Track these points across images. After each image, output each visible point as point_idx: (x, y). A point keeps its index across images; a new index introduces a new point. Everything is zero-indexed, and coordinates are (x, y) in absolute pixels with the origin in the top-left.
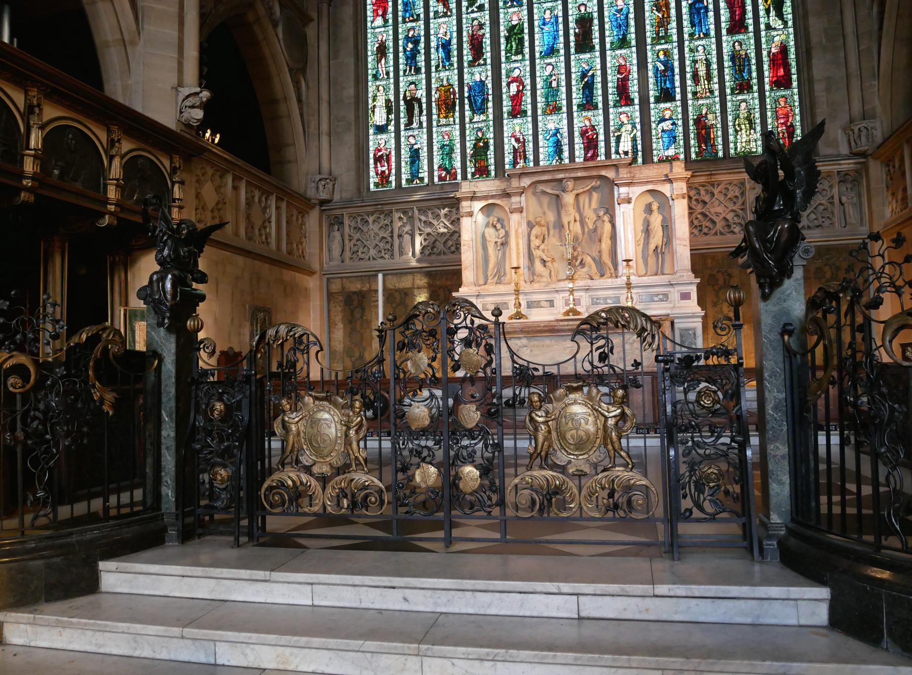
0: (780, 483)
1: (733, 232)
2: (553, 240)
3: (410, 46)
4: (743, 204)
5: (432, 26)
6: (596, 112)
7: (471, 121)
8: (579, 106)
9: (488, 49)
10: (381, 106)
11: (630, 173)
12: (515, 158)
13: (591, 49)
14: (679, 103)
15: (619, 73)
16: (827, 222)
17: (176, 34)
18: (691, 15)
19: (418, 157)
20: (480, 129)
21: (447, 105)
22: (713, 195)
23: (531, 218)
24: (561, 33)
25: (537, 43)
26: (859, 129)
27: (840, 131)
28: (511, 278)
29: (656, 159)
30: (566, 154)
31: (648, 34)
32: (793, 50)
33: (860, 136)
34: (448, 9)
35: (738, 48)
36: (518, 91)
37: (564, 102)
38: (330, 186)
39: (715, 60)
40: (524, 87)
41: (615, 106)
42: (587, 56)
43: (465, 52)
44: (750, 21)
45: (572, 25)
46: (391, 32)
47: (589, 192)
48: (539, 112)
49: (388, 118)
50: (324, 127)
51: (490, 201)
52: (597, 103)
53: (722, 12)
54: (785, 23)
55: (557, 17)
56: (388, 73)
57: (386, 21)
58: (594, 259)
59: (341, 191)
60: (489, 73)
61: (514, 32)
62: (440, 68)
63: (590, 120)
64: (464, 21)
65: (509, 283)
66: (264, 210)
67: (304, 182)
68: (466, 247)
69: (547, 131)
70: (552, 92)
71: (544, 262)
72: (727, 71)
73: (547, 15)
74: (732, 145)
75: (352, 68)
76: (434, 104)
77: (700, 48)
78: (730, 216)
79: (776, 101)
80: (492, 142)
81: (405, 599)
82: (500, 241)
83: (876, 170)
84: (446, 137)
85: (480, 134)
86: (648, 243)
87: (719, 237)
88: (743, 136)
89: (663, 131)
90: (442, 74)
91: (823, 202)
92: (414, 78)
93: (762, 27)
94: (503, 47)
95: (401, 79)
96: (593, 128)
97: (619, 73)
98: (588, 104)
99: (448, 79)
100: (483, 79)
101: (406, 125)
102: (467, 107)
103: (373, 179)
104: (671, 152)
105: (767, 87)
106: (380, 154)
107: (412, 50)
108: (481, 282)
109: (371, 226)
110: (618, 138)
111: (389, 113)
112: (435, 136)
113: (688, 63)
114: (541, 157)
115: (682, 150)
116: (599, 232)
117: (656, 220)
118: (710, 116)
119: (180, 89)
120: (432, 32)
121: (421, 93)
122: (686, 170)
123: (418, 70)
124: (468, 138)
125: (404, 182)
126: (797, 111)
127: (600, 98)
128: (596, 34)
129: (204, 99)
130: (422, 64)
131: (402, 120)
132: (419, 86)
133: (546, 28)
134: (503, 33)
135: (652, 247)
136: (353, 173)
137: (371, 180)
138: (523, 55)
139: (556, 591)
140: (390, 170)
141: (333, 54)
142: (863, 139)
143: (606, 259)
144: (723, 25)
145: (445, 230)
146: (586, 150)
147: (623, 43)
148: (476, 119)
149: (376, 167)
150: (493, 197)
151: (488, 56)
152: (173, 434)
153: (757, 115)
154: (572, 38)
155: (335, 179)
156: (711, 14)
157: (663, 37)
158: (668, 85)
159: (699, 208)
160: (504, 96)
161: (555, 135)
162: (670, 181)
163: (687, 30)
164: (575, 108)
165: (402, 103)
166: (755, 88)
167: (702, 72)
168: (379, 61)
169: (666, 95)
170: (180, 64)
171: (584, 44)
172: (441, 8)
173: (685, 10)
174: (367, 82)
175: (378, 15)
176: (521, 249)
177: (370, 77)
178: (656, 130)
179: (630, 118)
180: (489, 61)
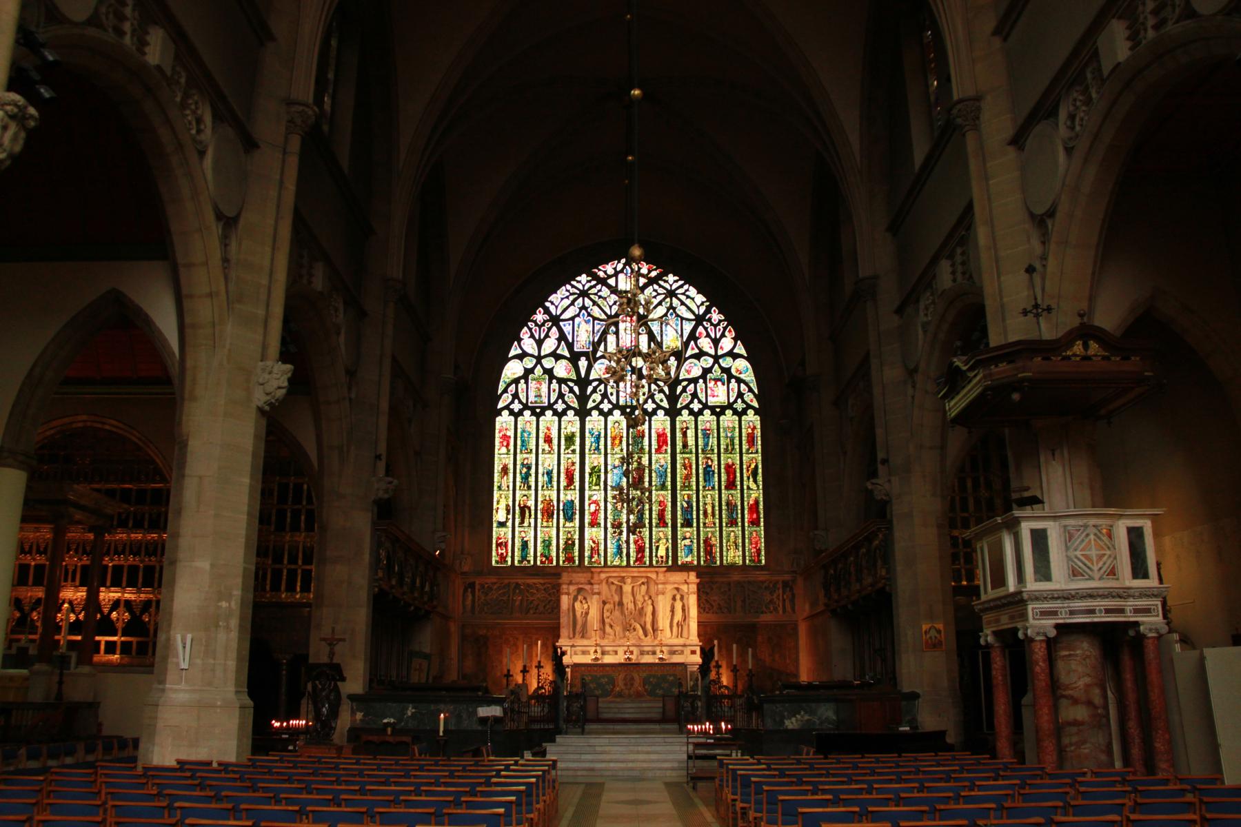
2: (617, 613)
3: (525, 470)
7: (564, 527)
12: (592, 554)
14: (695, 529)
15: (660, 506)
19: (527, 547)
20: (569, 532)
21: (548, 513)
22: (712, 589)
23: (604, 598)
29: (680, 563)
31: (678, 483)
32: (762, 503)
34: (552, 449)
35: (731, 498)
39: (717, 504)
41: (656, 527)
44: (739, 483)
47: (640, 585)
49: (507, 518)
51: (580, 586)
53: (723, 475)
54: (758, 486)
56: (508, 487)
57: (509, 451)
58: (641, 625)
62: (545, 488)
65: (589, 638)
71: (611, 626)
72: (724, 512)
74: (725, 558)
77: (709, 496)
85: (569, 536)
88: (731, 553)
89: (685, 545)
90: (546, 493)
92: (526, 493)
93: (745, 487)
101: (520, 524)
103: (494, 559)
104: (689, 559)
105: (746, 524)
106: (500, 541)
107: (526, 473)
108: (571, 636)
109: (494, 592)
110: (657, 548)
111: (508, 513)
113: (701, 504)
114: (609, 554)
115: (695, 558)
116: (645, 609)
117: (678, 605)
118: (713, 539)
120: (540, 463)
121: (531, 503)
123: (529, 488)
125: (516, 562)
126: (763, 540)
130: (533, 484)
134: (588, 470)
137: (493, 559)
143: (649, 627)
144: (723, 483)
146: (638, 552)
148: (568, 524)
149: (497, 550)
150: (582, 584)
151: (577, 484)
153: (740, 541)
156: (716, 475)
157: (687, 486)
158: (689, 517)
159: (704, 597)
160: (587, 512)
162: (688, 583)
163: (701, 483)
166: (740, 524)
167: (709, 511)
168: (502, 478)
169: (687, 523)
172: (547, 447)
173: (701, 471)
177: (495, 488)
178: (681, 544)
179: (666, 535)
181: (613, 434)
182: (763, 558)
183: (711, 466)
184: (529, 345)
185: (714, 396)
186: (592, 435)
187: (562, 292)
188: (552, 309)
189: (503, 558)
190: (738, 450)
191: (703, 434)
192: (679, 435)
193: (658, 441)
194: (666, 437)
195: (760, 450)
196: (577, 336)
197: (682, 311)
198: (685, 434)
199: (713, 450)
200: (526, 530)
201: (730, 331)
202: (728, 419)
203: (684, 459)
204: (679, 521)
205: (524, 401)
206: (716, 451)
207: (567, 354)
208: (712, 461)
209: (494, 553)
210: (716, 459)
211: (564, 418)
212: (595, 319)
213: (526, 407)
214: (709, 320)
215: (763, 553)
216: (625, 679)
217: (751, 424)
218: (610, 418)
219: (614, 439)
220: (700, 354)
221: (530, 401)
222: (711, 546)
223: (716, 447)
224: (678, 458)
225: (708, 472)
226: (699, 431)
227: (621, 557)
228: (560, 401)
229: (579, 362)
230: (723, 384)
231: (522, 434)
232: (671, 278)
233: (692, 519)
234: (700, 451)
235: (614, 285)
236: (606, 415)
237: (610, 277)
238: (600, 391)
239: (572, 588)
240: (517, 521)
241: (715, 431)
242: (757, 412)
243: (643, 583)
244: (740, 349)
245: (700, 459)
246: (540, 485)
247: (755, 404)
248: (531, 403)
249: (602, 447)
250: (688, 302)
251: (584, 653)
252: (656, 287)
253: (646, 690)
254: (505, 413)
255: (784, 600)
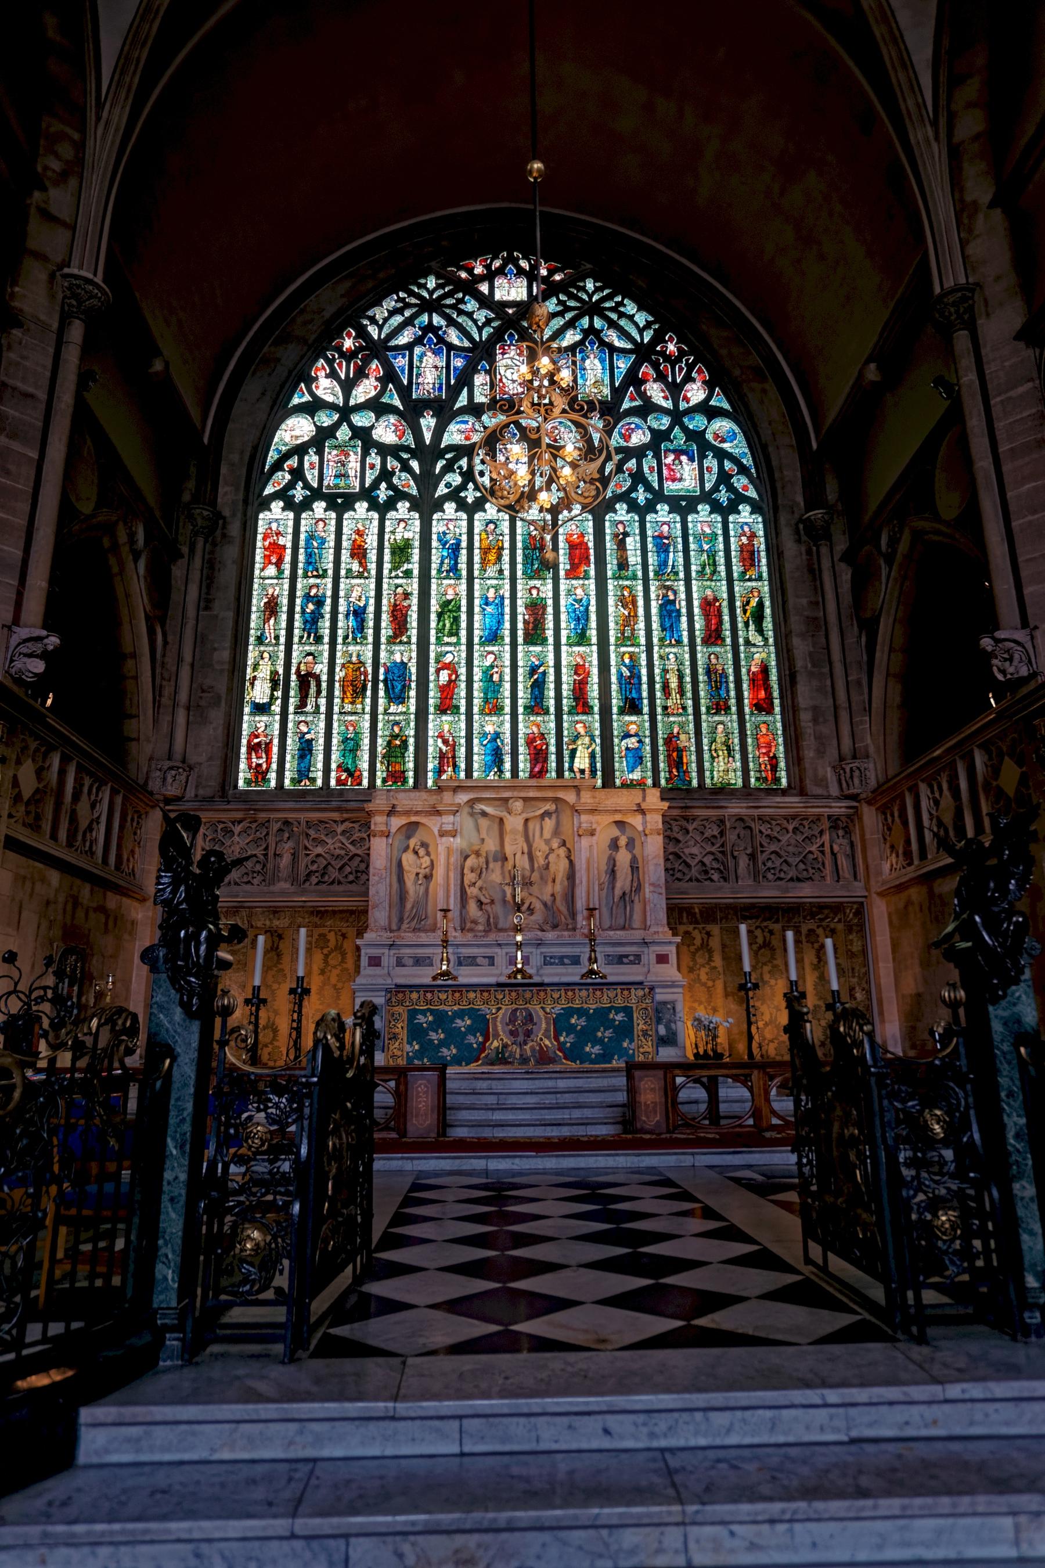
0: (1032, 1233)
1: (712, 880)
4: (722, 846)
5: (342, 586)
6: (546, 718)
7: (386, 712)
8: (526, 707)
9: (415, 624)
10: (264, 679)
11: (594, 797)
13: (544, 641)
14: (646, 717)
15: (576, 673)
16: (817, 877)
17: (19, 553)
18: (661, 616)
19: (310, 751)
20: (397, 723)
24: (507, 617)
25: (476, 625)
26: (851, 769)
27: (829, 769)
28: (435, 924)
29: (618, 782)
30: (507, 766)
31: (612, 633)
33: (852, 777)
34: (365, 569)
35: (714, 661)
36: (450, 681)
37: (508, 702)
38: (183, 778)
39: (688, 671)
40: (457, 676)
41: (570, 713)
42: (538, 649)
43: (383, 624)
44: (728, 633)
45: (521, 610)
46: (286, 586)
47: (543, 816)
48: (476, 710)
49: (272, 695)
50: (183, 697)
51: (414, 819)
52: (548, 709)
53: (696, 618)
54: (766, 640)
55: (502, 598)
56: (277, 638)
57: (280, 571)
58: (545, 904)
59: (197, 787)
60: (414, 655)
61: (448, 607)
63: (538, 726)
64: (385, 586)
65: (434, 930)
66: (93, 806)
67: (145, 770)
68: (376, 878)
69: (485, 735)
70: (492, 686)
71: (480, 904)
72: (701, 685)
73: (491, 594)
74: (707, 774)
75: (230, 624)
76: (337, 685)
77: (671, 656)
78: (707, 860)
79: (757, 727)
80: (411, 741)
81: (607, 1432)
82: (422, 872)
83: (870, 816)
84: (351, 728)
85: (396, 729)
86: (613, 888)
87: (695, 883)
88: (721, 764)
89: (627, 749)
90: (351, 648)
91: (814, 848)
93: (741, 641)
94: (433, 625)
95: (295, 647)
96: (542, 736)
97: (576, 673)
98: (537, 706)
99: (358, 656)
100: (405, 660)
101: (297, 707)
102: (381, 693)
103: (243, 774)
104: (636, 776)
105: (747, 710)
107: (313, 612)
108: (394, 927)
109: (236, 838)
110: (573, 753)
111: (274, 689)
112: (335, 725)
113: (657, 671)
114: (476, 766)
115: (649, 774)
116: (552, 868)
117: (623, 857)
118: (683, 737)
119: (15, 628)
120: (342, 594)
121: (321, 668)
122: (662, 799)
123: (319, 640)
124: (380, 733)
125: (287, 782)
126: (780, 740)
127: (552, 702)
128: (550, 624)
129: (50, 648)
130: (326, 632)
131: (291, 700)
132: (319, 659)
133: (489, 609)
134: (434, 607)
135: (618, 892)
136: (218, 762)
137: (241, 775)
138: (459, 639)
139: (819, 1401)
140: (269, 762)
141: (206, 603)
142: (856, 781)
144: (697, 633)
145: (343, 852)
147: (582, 638)
148: (393, 709)
149: (249, 759)
150: (417, 813)
151: (414, 633)
152: (183, 1177)
153: (736, 741)
154: (520, 625)
155: (191, 768)
156: (684, 619)
158: (634, 695)
160: (431, 685)
161: (495, 740)
162: (641, 811)
164: (521, 710)
165: (293, 677)
166: (734, 709)
167: (674, 684)
168: (266, 621)
169: (632, 707)
170: (20, 595)
171: (534, 635)
172: (356, 567)
173: (654, 611)
174: (247, 644)
175: (270, 563)
176: (452, 886)
177: (252, 640)
178: (620, 746)
180: (414, 639)
181: (485, 544)
182: (783, 774)
183: (674, 601)
184: (326, 388)
185: (673, 480)
186: (444, 545)
187: (390, 303)
188: (373, 331)
189: (260, 774)
190: (723, 574)
191: (656, 545)
192: (610, 544)
193: (571, 558)
194: (588, 549)
195: (765, 575)
196: (418, 375)
197: (613, 337)
198: (621, 545)
199: (676, 574)
200: (310, 718)
201: (700, 371)
202: (703, 518)
203: (623, 588)
204: (615, 703)
205: (315, 485)
206: (682, 575)
207: (397, 402)
208: (675, 593)
209: (243, 765)
210: (682, 589)
211: (391, 514)
212: (451, 347)
213: (317, 494)
214: (663, 353)
215: (782, 764)
216: (512, 1020)
217: (746, 528)
218: (478, 516)
219: (485, 551)
220: (647, 409)
221: (325, 483)
222: (680, 751)
223: (681, 568)
224: (610, 587)
225: (668, 610)
226: (649, 539)
227: (501, 771)
228: (383, 485)
229: (423, 422)
230: (691, 459)
231: (307, 541)
232: (590, 285)
233: (641, 698)
234: (651, 575)
235: (486, 292)
236: (471, 509)
237: (481, 278)
238: (460, 468)
239: (396, 822)
240: (293, 702)
241: (680, 540)
242: (756, 509)
243: (547, 814)
244: (719, 401)
245: (653, 588)
246: (340, 632)
247: (752, 493)
248: (328, 486)
249: (463, 566)
250: (623, 322)
251: (418, 961)
252: (562, 297)
253: (561, 1047)
254: (277, 506)
255: (834, 854)
